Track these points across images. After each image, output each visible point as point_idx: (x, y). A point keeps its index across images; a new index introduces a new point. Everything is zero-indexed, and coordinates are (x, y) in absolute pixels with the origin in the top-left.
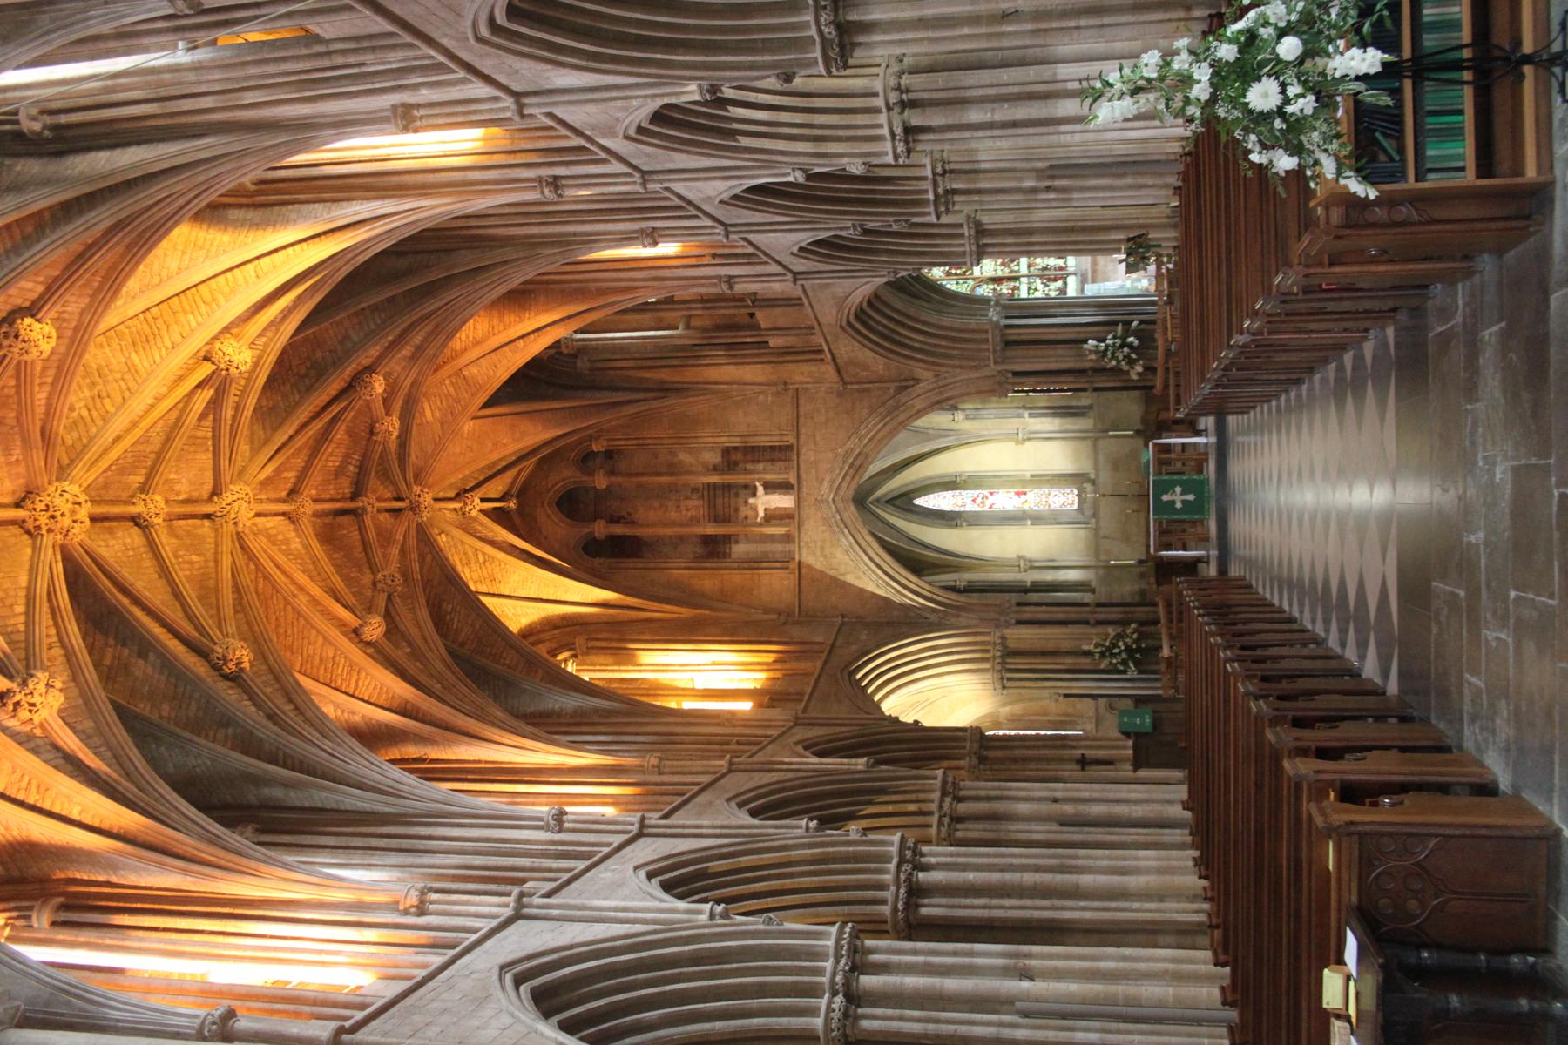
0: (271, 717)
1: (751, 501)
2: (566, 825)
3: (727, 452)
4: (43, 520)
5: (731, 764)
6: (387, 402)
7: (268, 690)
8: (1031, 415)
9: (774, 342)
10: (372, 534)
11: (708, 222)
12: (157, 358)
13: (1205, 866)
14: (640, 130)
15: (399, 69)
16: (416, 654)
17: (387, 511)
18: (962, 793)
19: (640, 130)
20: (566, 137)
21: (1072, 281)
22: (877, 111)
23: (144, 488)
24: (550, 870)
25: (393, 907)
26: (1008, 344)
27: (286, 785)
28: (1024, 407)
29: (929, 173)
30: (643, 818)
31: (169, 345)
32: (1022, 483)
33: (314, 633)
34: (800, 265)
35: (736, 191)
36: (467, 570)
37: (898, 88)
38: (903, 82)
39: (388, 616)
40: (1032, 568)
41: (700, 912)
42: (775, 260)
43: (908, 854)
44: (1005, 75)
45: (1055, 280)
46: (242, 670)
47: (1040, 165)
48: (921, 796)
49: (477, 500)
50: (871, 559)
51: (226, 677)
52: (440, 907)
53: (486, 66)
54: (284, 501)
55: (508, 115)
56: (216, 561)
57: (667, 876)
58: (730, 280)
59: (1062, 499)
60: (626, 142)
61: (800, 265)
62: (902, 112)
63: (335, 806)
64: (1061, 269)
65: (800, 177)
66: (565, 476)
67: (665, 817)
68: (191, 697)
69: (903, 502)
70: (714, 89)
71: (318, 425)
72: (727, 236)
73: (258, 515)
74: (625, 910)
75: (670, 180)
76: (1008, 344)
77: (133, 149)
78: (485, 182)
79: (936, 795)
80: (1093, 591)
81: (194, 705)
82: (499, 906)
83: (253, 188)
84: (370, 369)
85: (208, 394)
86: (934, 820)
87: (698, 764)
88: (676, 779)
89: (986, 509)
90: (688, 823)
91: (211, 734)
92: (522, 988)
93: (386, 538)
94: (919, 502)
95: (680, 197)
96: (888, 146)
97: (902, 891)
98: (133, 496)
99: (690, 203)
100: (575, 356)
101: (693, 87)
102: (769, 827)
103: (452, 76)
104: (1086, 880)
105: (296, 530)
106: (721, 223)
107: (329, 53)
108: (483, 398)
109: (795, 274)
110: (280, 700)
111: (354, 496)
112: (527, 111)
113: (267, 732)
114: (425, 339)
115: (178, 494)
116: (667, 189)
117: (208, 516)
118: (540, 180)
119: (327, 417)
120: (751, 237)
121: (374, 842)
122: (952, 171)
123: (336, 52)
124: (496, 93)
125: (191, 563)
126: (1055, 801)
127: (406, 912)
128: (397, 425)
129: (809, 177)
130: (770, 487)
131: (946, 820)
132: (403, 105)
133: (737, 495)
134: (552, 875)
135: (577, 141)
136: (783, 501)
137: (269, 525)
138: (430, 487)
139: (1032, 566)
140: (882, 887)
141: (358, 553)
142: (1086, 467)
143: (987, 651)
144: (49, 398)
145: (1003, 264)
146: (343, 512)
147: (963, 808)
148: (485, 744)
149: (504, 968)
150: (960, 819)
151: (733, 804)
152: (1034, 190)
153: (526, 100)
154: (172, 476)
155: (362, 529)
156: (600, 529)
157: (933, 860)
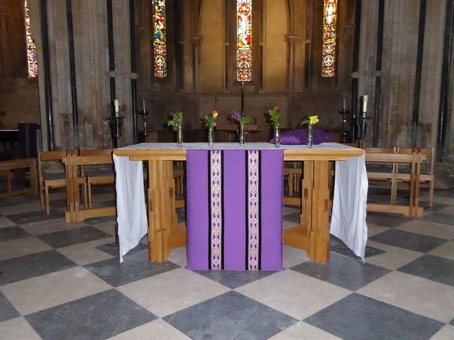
8: (307, 45)
28: (313, 40)
32: (256, 38)
40: (194, 46)
80: (177, 91)
89: (238, 14)
139: (196, 44)
142: (267, 87)
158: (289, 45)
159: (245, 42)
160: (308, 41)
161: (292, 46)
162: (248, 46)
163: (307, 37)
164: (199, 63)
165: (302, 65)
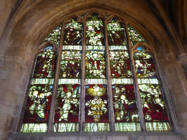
21: (42, 128)
45: (47, 111)
64: (57, 116)
145: (70, 65)
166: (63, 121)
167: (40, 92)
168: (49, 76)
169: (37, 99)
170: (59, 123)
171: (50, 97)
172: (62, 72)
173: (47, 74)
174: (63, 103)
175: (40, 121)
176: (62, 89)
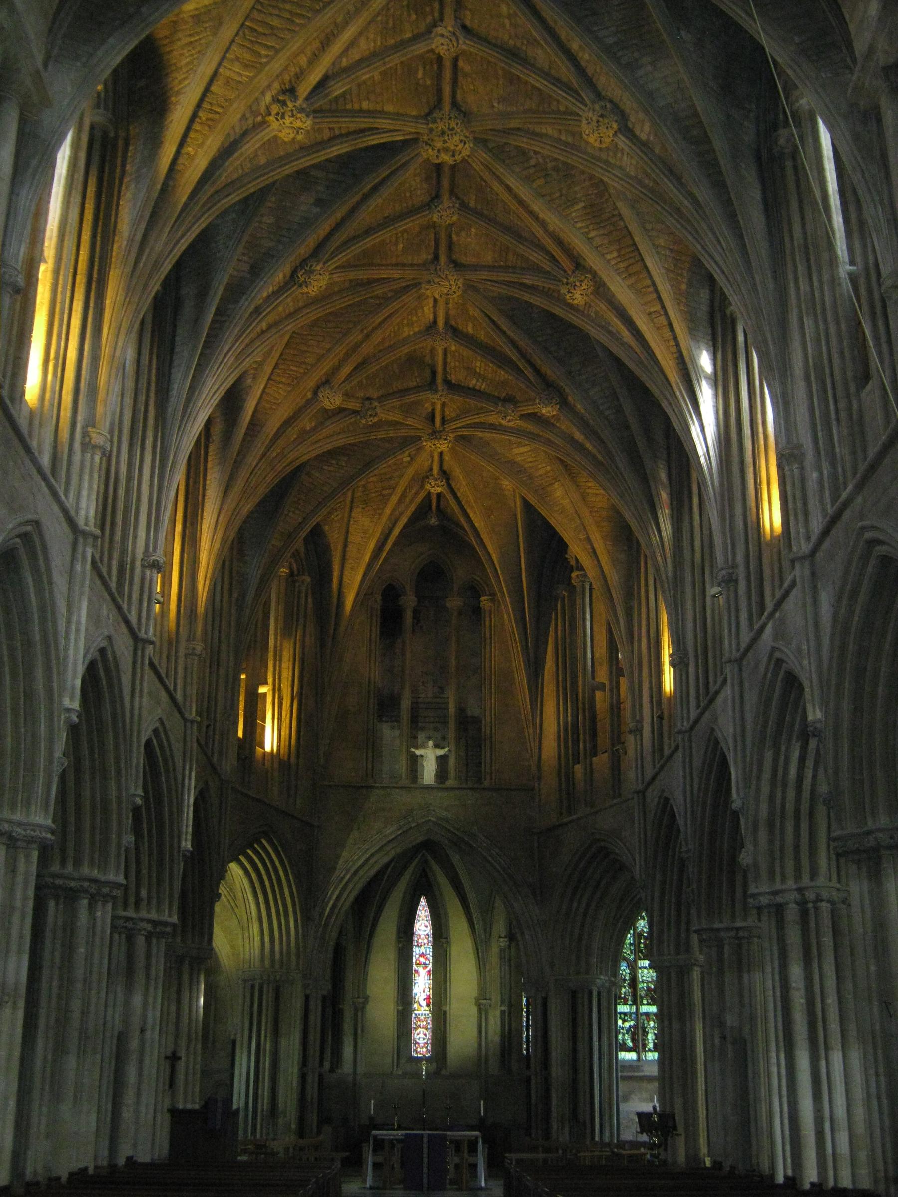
0: (257, 311)
1: (430, 743)
2: (148, 572)
3: (477, 721)
4: (441, 126)
5: (192, 722)
6: (534, 417)
7: (281, 309)
8: (503, 1013)
9: (578, 768)
10: (412, 398)
11: (694, 714)
12: (579, 225)
13: (79, 1177)
14: (779, 662)
15: (834, 455)
16: (304, 435)
17: (433, 410)
18: (154, 941)
19: (779, 662)
20: (773, 595)
21: (632, 1056)
22: (798, 877)
23: (464, 206)
24: (110, 558)
25: (91, 422)
26: (574, 994)
27: (196, 321)
28: (510, 1006)
29: (739, 924)
30: (152, 643)
31: (590, 236)
33: (328, 346)
34: (652, 795)
35: (723, 744)
36: (374, 479)
37: (819, 899)
38: (824, 904)
39: (340, 411)
40: (356, 1010)
41: (72, 698)
42: (657, 774)
43: (105, 890)
44: (832, 1000)
45: (633, 1040)
46: (301, 286)
47: (746, 1030)
48: (154, 901)
49: (439, 490)
50: (372, 855)
51: (294, 273)
52: (88, 464)
53: (838, 531)
54: (446, 323)
55: (795, 548)
56: (397, 265)
57: (100, 665)
58: (638, 731)
59: (421, 1042)
60: (769, 649)
61: (652, 795)
62: (797, 903)
63: (176, 362)
64: (644, 1046)
65: (735, 806)
66: (461, 573)
67: (151, 664)
68: (279, 242)
69: (423, 886)
70: (817, 734)
71: (514, 356)
72: (679, 732)
73: (435, 300)
74: (78, 631)
75: (733, 685)
76: (574, 994)
77: (762, 219)
78: (732, 516)
79: (153, 915)
80: (332, 1070)
81: (271, 244)
82: (87, 518)
83: (728, 312)
84: (564, 403)
85: (547, 266)
86: (131, 913)
87: (193, 691)
88: (180, 671)
89: (414, 966)
90: (145, 684)
91: (246, 258)
92: (18, 540)
93: (408, 410)
94: (423, 902)
95: (717, 693)
96: (764, 888)
97: (73, 884)
98: (458, 198)
99: (712, 701)
100: (569, 583)
101: (819, 715)
102: (138, 758)
103: (828, 501)
104: (71, 1062)
105: (420, 332)
106: (692, 728)
107: (848, 396)
108: (533, 501)
109: (642, 793)
110: (271, 318)
111: (448, 383)
112: (798, 566)
113: (247, 305)
114: (589, 452)
115: (458, 235)
116: (725, 680)
117: (436, 258)
118: (734, 566)
119: (521, 364)
120: (680, 754)
121: (142, 398)
122: (740, 946)
123: (850, 402)
124: (814, 538)
125: (396, 244)
126: (142, 1031)
127: (85, 434)
128: (511, 424)
129: (736, 815)
130: (442, 761)
131: (130, 925)
132: (803, 454)
133: (436, 729)
134: (106, 560)
135: (769, 605)
136: (429, 771)
137: (425, 309)
138: (453, 449)
139: (360, 1009)
140: (78, 863)
141: (397, 385)
143: (281, 967)
144: (546, 135)
145: (648, 988)
146: (434, 373)
147: (141, 941)
148: (221, 495)
149: (37, 523)
150: (130, 939)
151: (157, 724)
152: (722, 1024)
153: (807, 563)
154: (473, 230)
155: (418, 388)
156: (409, 601)
157: (99, 914)
158: (480, 1010)
159: (424, 1004)
160: (503, 1008)
161: (484, 1013)
162: (427, 1009)
163: (502, 1003)
164: (362, 1031)
165: (497, 1039)
166: (650, 1050)
167: (624, 1021)
168: (630, 1003)
169: (622, 1029)
170: (645, 1051)
171: (636, 1027)
172: (642, 998)
173: (627, 1000)
174: (647, 1033)
175: (629, 1050)
176: (644, 1017)
